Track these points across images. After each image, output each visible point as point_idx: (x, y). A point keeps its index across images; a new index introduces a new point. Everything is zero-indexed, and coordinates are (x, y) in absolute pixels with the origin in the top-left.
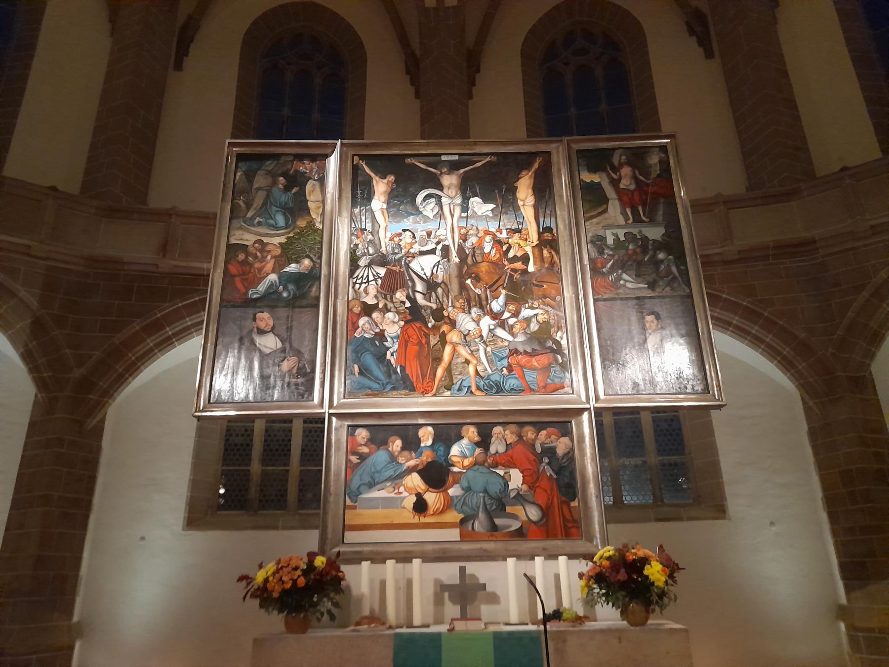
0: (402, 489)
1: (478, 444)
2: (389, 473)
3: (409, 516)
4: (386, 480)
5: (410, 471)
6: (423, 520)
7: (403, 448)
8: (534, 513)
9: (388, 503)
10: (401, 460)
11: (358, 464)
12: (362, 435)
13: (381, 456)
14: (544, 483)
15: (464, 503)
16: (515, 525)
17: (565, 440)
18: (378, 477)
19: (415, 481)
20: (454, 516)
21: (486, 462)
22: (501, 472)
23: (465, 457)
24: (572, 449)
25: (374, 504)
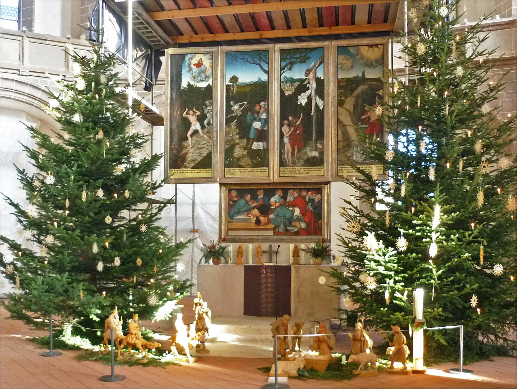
0: (250, 215)
2: (245, 209)
3: (254, 226)
4: (244, 211)
5: (254, 208)
6: (259, 227)
7: (251, 199)
8: (303, 225)
9: (244, 220)
10: (250, 203)
11: (233, 205)
12: (234, 193)
13: (242, 202)
14: (308, 214)
15: (275, 221)
16: (296, 230)
17: (319, 196)
18: (241, 210)
19: (256, 212)
20: (271, 226)
22: (291, 209)
23: (276, 203)
24: (321, 199)
25: (240, 220)
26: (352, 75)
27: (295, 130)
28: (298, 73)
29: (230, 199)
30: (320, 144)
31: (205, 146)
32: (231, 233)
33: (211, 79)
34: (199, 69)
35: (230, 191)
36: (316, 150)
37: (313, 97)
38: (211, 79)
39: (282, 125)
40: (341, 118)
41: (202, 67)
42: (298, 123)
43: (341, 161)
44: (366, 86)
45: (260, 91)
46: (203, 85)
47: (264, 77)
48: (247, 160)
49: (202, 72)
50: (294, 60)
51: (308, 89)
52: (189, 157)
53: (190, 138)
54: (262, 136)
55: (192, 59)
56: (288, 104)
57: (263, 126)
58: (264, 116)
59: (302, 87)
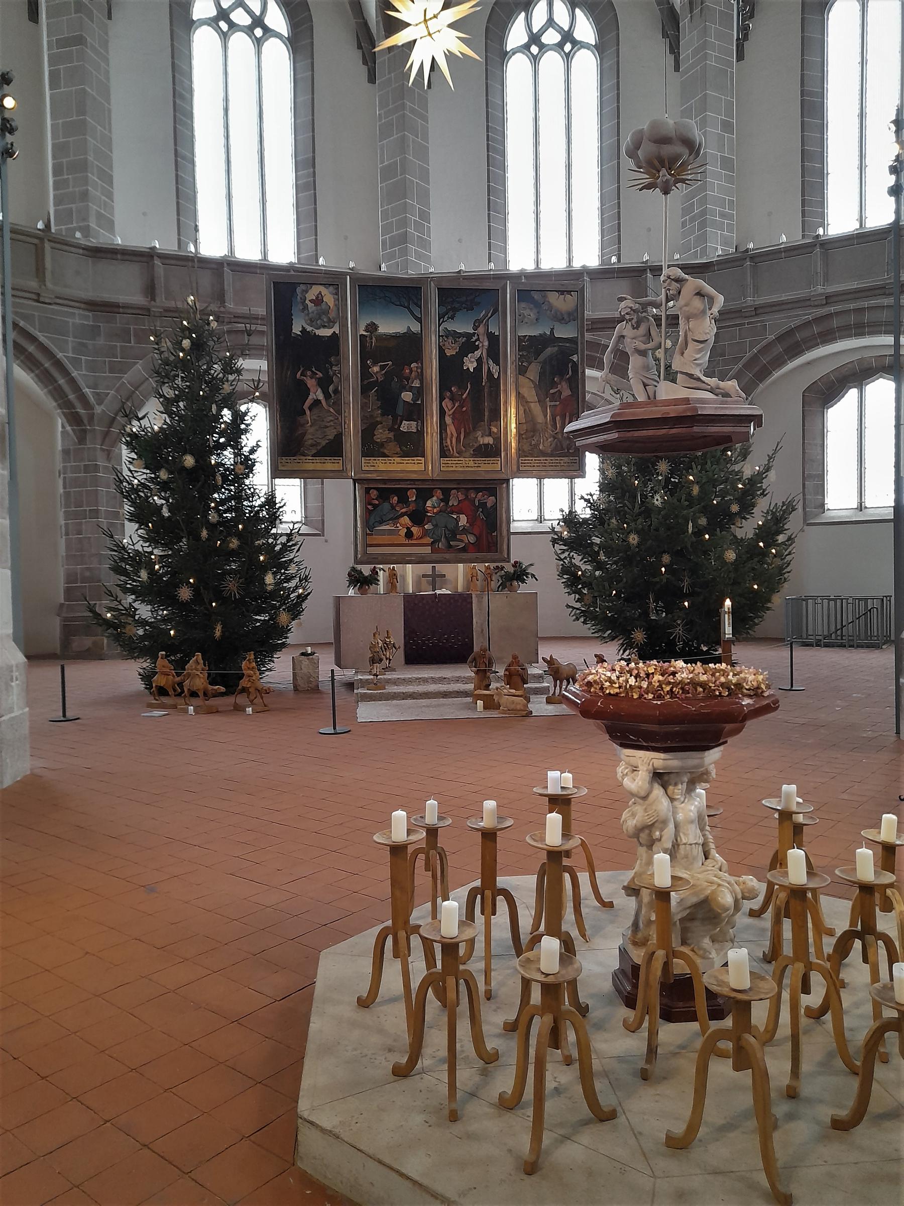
1: (442, 500)
2: (392, 516)
5: (403, 515)
6: (411, 542)
8: (472, 539)
12: (374, 494)
13: (386, 506)
16: (462, 545)
19: (406, 520)
20: (429, 540)
21: (447, 510)
27: (461, 406)
28: (462, 326)
29: (368, 502)
30: (496, 426)
31: (332, 423)
32: (370, 550)
33: (337, 325)
34: (319, 308)
35: (367, 490)
36: (490, 435)
37: (485, 360)
38: (337, 325)
39: (442, 398)
40: (525, 391)
41: (323, 306)
42: (464, 396)
43: (524, 451)
44: (556, 349)
45: (409, 347)
46: (326, 332)
47: (416, 327)
48: (393, 447)
49: (324, 313)
50: (457, 305)
51: (477, 348)
52: (309, 439)
53: (308, 412)
54: (416, 412)
55: (307, 292)
56: (450, 369)
57: (415, 399)
58: (416, 384)
59: (469, 346)
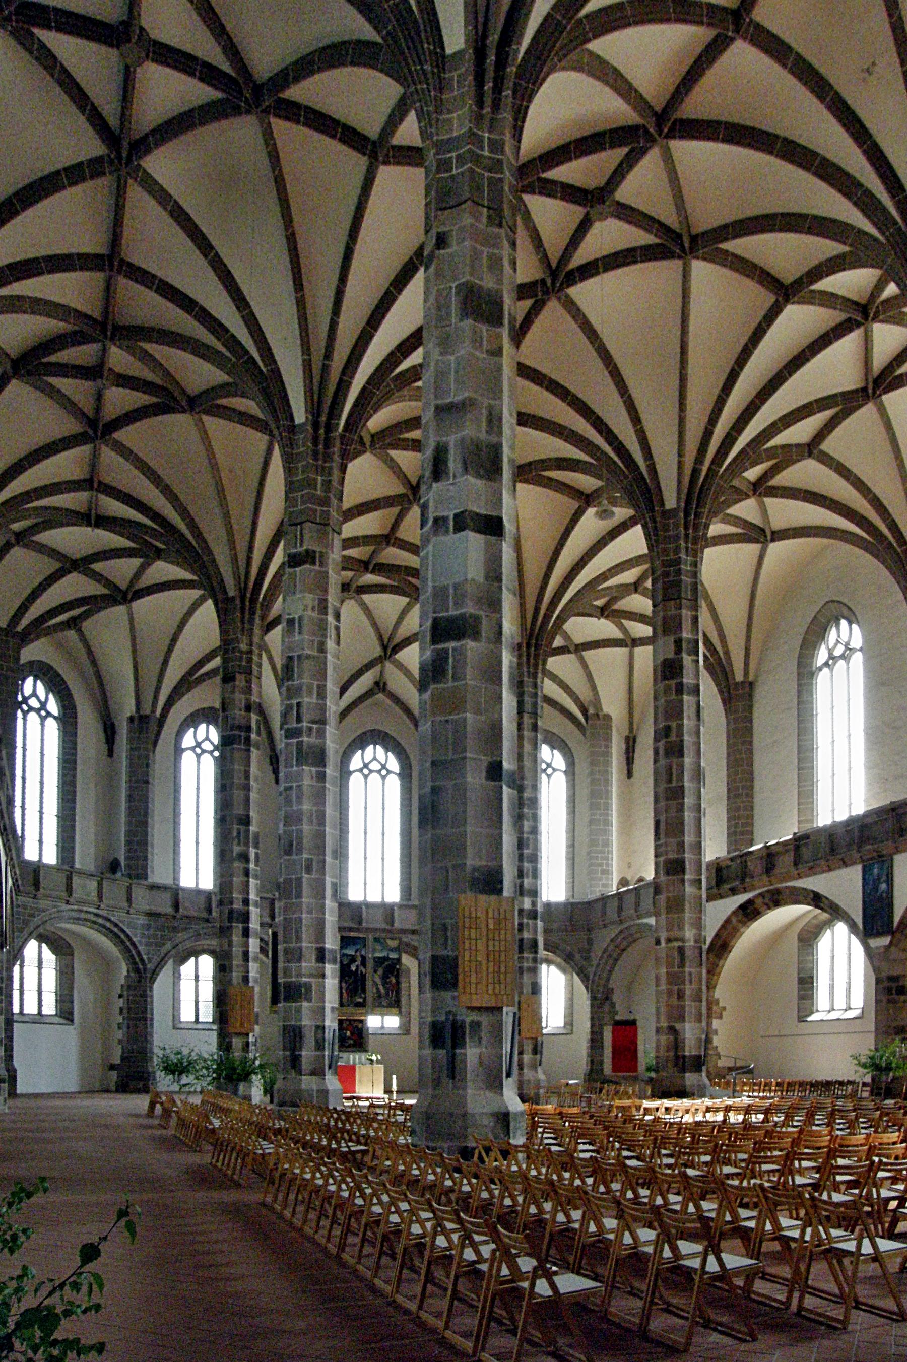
26: (381, 955)
28: (350, 952)
59: (353, 960)
